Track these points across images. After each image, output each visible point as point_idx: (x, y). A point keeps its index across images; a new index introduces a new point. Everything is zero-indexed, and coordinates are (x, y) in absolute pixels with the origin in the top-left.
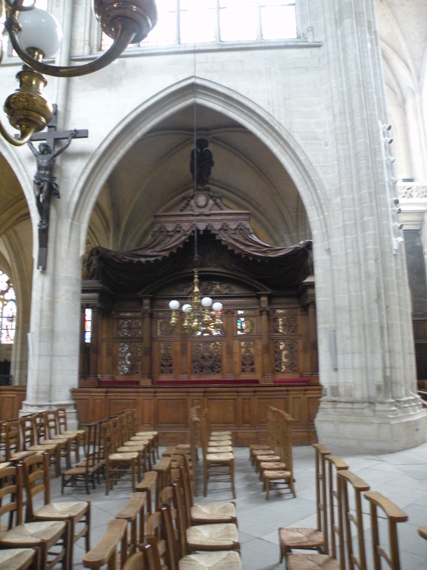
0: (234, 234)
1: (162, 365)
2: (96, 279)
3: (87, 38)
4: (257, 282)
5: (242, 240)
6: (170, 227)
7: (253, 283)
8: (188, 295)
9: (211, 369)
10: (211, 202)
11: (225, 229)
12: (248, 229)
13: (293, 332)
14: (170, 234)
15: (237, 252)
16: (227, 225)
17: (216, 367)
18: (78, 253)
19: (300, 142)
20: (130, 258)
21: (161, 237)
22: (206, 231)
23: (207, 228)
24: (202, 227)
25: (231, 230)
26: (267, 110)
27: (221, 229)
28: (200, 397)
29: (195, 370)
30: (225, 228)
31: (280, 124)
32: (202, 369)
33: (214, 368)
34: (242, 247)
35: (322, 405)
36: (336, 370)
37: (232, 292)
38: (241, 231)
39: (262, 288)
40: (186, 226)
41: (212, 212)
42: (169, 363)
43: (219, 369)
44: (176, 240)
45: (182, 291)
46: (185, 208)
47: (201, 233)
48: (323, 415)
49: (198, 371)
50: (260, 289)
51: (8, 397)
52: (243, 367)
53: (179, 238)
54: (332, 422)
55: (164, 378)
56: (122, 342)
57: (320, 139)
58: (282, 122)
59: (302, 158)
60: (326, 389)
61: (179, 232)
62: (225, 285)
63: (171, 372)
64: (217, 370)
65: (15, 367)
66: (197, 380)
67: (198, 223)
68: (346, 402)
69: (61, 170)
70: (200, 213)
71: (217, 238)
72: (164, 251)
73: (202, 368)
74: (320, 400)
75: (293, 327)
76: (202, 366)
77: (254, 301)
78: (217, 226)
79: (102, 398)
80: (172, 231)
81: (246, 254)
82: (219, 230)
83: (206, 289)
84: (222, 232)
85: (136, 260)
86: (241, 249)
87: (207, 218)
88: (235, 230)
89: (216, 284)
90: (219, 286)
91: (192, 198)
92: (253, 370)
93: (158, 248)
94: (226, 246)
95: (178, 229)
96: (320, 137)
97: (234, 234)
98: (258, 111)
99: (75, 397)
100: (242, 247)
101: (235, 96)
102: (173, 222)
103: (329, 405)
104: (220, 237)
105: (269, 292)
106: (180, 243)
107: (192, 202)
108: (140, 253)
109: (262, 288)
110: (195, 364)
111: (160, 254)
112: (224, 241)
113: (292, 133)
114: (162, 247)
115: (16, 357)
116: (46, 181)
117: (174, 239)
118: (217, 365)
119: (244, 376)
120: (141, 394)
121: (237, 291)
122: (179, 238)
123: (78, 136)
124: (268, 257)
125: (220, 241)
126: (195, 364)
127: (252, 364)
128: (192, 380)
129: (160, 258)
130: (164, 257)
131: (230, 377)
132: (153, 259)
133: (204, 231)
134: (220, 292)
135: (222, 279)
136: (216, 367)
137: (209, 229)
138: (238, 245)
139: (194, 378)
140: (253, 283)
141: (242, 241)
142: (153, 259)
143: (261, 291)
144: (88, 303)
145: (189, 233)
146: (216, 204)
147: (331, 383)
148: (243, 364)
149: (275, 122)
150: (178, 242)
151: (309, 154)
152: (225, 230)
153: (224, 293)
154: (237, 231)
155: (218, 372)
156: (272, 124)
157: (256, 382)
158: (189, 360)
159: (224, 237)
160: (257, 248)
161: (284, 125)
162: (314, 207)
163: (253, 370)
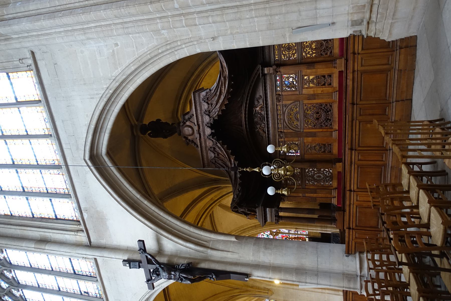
0: (212, 104)
1: (324, 152)
2: (256, 209)
3: (73, 233)
6: (211, 155)
8: (265, 133)
9: (328, 112)
10: (188, 123)
11: (208, 113)
12: (207, 93)
14: (216, 155)
15: (227, 102)
16: (205, 110)
18: (234, 242)
19: (120, 70)
20: (238, 185)
22: (212, 127)
24: (208, 131)
25: (209, 107)
26: (98, 100)
27: (209, 115)
31: (107, 88)
32: (328, 119)
33: (327, 109)
34: (222, 97)
35: (372, 34)
36: (333, 23)
37: (261, 97)
38: (209, 99)
39: (256, 74)
40: (210, 143)
41: (196, 123)
45: (262, 137)
47: (213, 131)
48: (382, 33)
51: (352, 297)
52: (326, 84)
53: (219, 148)
54: (392, 25)
55: (335, 150)
56: (305, 182)
57: (113, 51)
58: (105, 86)
59: (133, 68)
60: (354, 32)
61: (214, 148)
62: (256, 103)
63: (331, 144)
64: (330, 108)
65: (325, 231)
66: (337, 125)
68: (371, 11)
69: (172, 256)
71: (216, 118)
72: (230, 161)
73: (327, 120)
74: (365, 37)
77: (268, 78)
78: (207, 119)
79: (354, 232)
80: (214, 154)
81: (228, 95)
82: (210, 118)
83: (260, 119)
84: (211, 114)
86: (224, 99)
89: (256, 110)
90: (257, 107)
91: (186, 138)
92: (330, 76)
94: (223, 111)
95: (212, 149)
96: (111, 51)
98: (101, 107)
100: (222, 97)
101: (93, 127)
103: (372, 27)
104: (216, 116)
105: (260, 67)
106: (223, 147)
107: (190, 138)
108: (233, 177)
109: (256, 74)
110: (323, 125)
113: (114, 78)
115: (318, 230)
116: (179, 274)
117: (220, 152)
119: (335, 83)
120: (352, 202)
121: (260, 92)
122: (219, 148)
123: (143, 248)
126: (323, 125)
127: (324, 76)
128: (337, 128)
130: (235, 160)
131: (336, 97)
134: (262, 107)
135: (252, 106)
137: (209, 125)
138: (221, 101)
139: (336, 127)
140: (252, 82)
141: (217, 97)
143: (260, 73)
144: (274, 216)
145: (214, 141)
146: (189, 119)
147: (348, 26)
148: (324, 85)
149: (107, 92)
151: (128, 62)
152: (209, 113)
153: (262, 103)
154: (209, 102)
155: (331, 106)
156: (108, 96)
157: (341, 73)
158: (321, 130)
159: (215, 112)
160: (222, 85)
161: (108, 85)
162: (176, 53)
163: (330, 76)
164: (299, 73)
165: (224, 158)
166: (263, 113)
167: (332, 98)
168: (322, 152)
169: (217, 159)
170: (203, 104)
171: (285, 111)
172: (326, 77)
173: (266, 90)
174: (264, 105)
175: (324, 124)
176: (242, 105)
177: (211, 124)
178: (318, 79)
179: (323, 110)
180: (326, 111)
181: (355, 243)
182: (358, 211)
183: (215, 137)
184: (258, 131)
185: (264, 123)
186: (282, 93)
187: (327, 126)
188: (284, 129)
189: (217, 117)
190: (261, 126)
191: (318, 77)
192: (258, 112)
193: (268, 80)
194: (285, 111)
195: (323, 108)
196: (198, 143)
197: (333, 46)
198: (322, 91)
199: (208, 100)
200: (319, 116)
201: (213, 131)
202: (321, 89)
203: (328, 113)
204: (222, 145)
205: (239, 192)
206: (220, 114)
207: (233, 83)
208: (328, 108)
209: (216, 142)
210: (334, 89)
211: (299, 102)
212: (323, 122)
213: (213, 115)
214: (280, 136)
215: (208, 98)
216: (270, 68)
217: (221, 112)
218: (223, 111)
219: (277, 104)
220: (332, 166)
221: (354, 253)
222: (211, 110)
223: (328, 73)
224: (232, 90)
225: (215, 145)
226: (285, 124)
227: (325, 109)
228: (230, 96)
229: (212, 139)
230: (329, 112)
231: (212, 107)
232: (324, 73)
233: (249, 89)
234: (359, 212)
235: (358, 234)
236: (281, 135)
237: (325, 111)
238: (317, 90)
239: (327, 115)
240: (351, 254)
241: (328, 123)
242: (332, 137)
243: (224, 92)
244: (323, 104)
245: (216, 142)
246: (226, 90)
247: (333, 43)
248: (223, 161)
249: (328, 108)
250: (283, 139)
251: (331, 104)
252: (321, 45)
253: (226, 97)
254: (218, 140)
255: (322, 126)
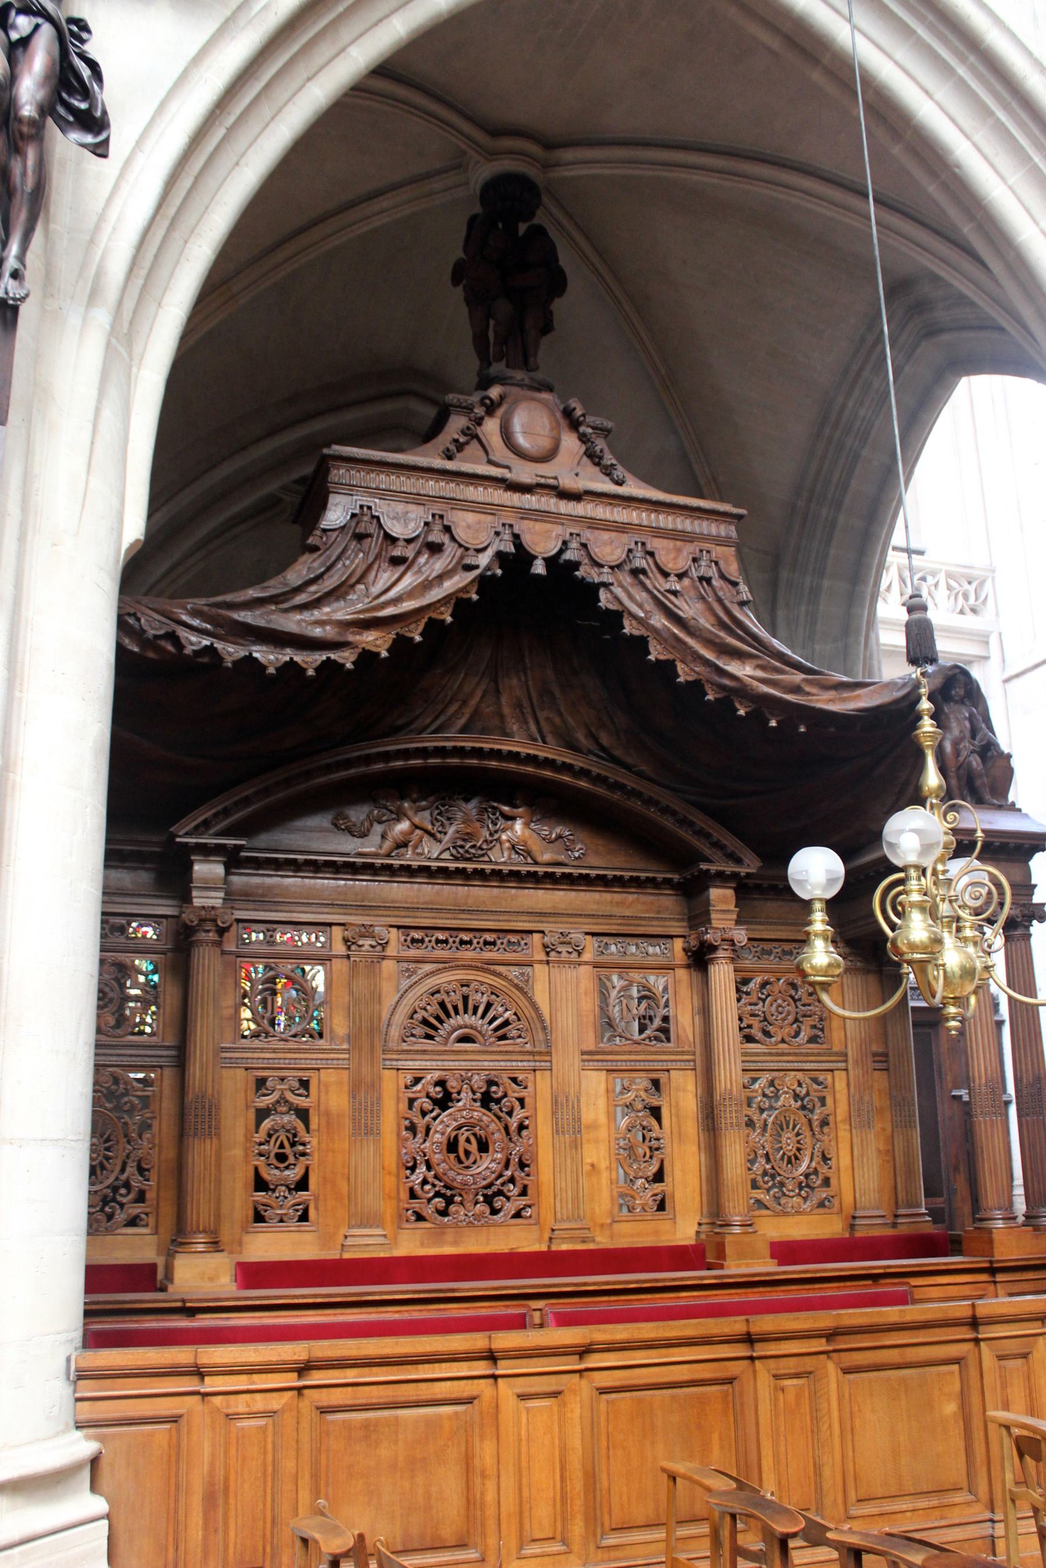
1: (261, 1184)
4: (700, 820)
5: (705, 623)
7: (684, 822)
8: (388, 855)
9: (488, 1200)
10: (570, 442)
12: (735, 584)
13: (813, 1039)
15: (684, 673)
17: (513, 1190)
21: (356, 561)
23: (561, 552)
28: (809, 1363)
29: (416, 1204)
30: (639, 562)
32: (449, 1201)
33: (500, 1193)
38: (704, 589)
39: (717, 845)
42: (294, 1175)
43: (522, 1201)
44: (426, 586)
45: (364, 835)
46: (460, 447)
47: (539, 568)
49: (428, 1211)
50: (707, 851)
53: (441, 578)
61: (435, 549)
64: (511, 1207)
67: (527, 524)
70: (543, 481)
75: (809, 1021)
76: (446, 1187)
77: (668, 902)
80: (409, 541)
81: (723, 688)
82: (612, 568)
84: (627, 579)
85: (231, 651)
87: (566, 507)
88: (680, 576)
89: (513, 818)
90: (527, 825)
93: (341, 611)
95: (436, 536)
97: (675, 593)
99: (87, 1411)
102: (417, 499)
107: (491, 427)
109: (717, 845)
110: (417, 1178)
111: (351, 638)
112: (634, 617)
114: (360, 606)
118: (512, 1180)
122: (441, 578)
124: (813, 708)
125: (616, 617)
126: (417, 1178)
127: (659, 1177)
129: (347, 658)
130: (367, 657)
132: (321, 657)
133: (551, 562)
136: (513, 1190)
140: (684, 822)
142: (320, 657)
143: (709, 861)
145: (484, 560)
150: (435, 594)
152: (636, 572)
154: (686, 581)
155: (518, 1215)
158: (391, 1161)
164: (677, 1053)
165: (375, 590)
166: (495, 855)
167: (562, 1220)
168: (256, 1169)
169: (374, 551)
170: (679, 551)
171: (499, 975)
172: (658, 1187)
173: (570, 881)
174: (536, 863)
175: (425, 1182)
176: (573, 746)
177: (576, 565)
178: (650, 1148)
179: (500, 1176)
180: (494, 1188)
181: (174, 1419)
182: (439, 1417)
183: (499, 572)
184: (399, 818)
185: (440, 854)
186: (586, 963)
187: (413, 1195)
188: (399, 960)
189: (611, 607)
190: (426, 838)
191: (657, 1149)
192: (504, 830)
193: (652, 898)
194: (499, 975)
195: (509, 1173)
196: (464, 460)
197: (785, 1214)
198: (593, 1165)
199: (701, 579)
200: (467, 1153)
201: (539, 568)
202: (603, 1164)
203: (481, 1199)
204: (459, 603)
205: (156, 637)
206: (626, 622)
207: (773, 723)
208: (508, 1198)
209: (477, 567)
210: (602, 1225)
211: (543, 1049)
212: (436, 1177)
213: (621, 586)
214: (362, 936)
215: (708, 580)
216: (735, 917)
217: (636, 633)
218: (641, 643)
219: (536, 937)
220: (204, 1231)
221: (82, 1417)
222: (647, 582)
223: (677, 1195)
224: (742, 712)
225: (462, 558)
226: (428, 967)
227: (503, 1184)
228: (710, 697)
229: (490, 552)
230: (482, 1208)
231: (668, 591)
232: (678, 1174)
233: (650, 802)
234: (432, 1424)
235: (263, 1429)
236: (367, 942)
237: (490, 1185)
238: (597, 1141)
239: (471, 1196)
240: (75, 1391)
241: (429, 1200)
242: (353, 1227)
243: (744, 671)
244: (528, 1175)
245: (477, 567)
246: (755, 683)
247: (798, 1213)
248: (358, 582)
249: (508, 1198)
250: (339, 948)
251: (530, 1217)
252: (789, 1162)
253: (717, 678)
254: (484, 582)
255: (413, 1169)
